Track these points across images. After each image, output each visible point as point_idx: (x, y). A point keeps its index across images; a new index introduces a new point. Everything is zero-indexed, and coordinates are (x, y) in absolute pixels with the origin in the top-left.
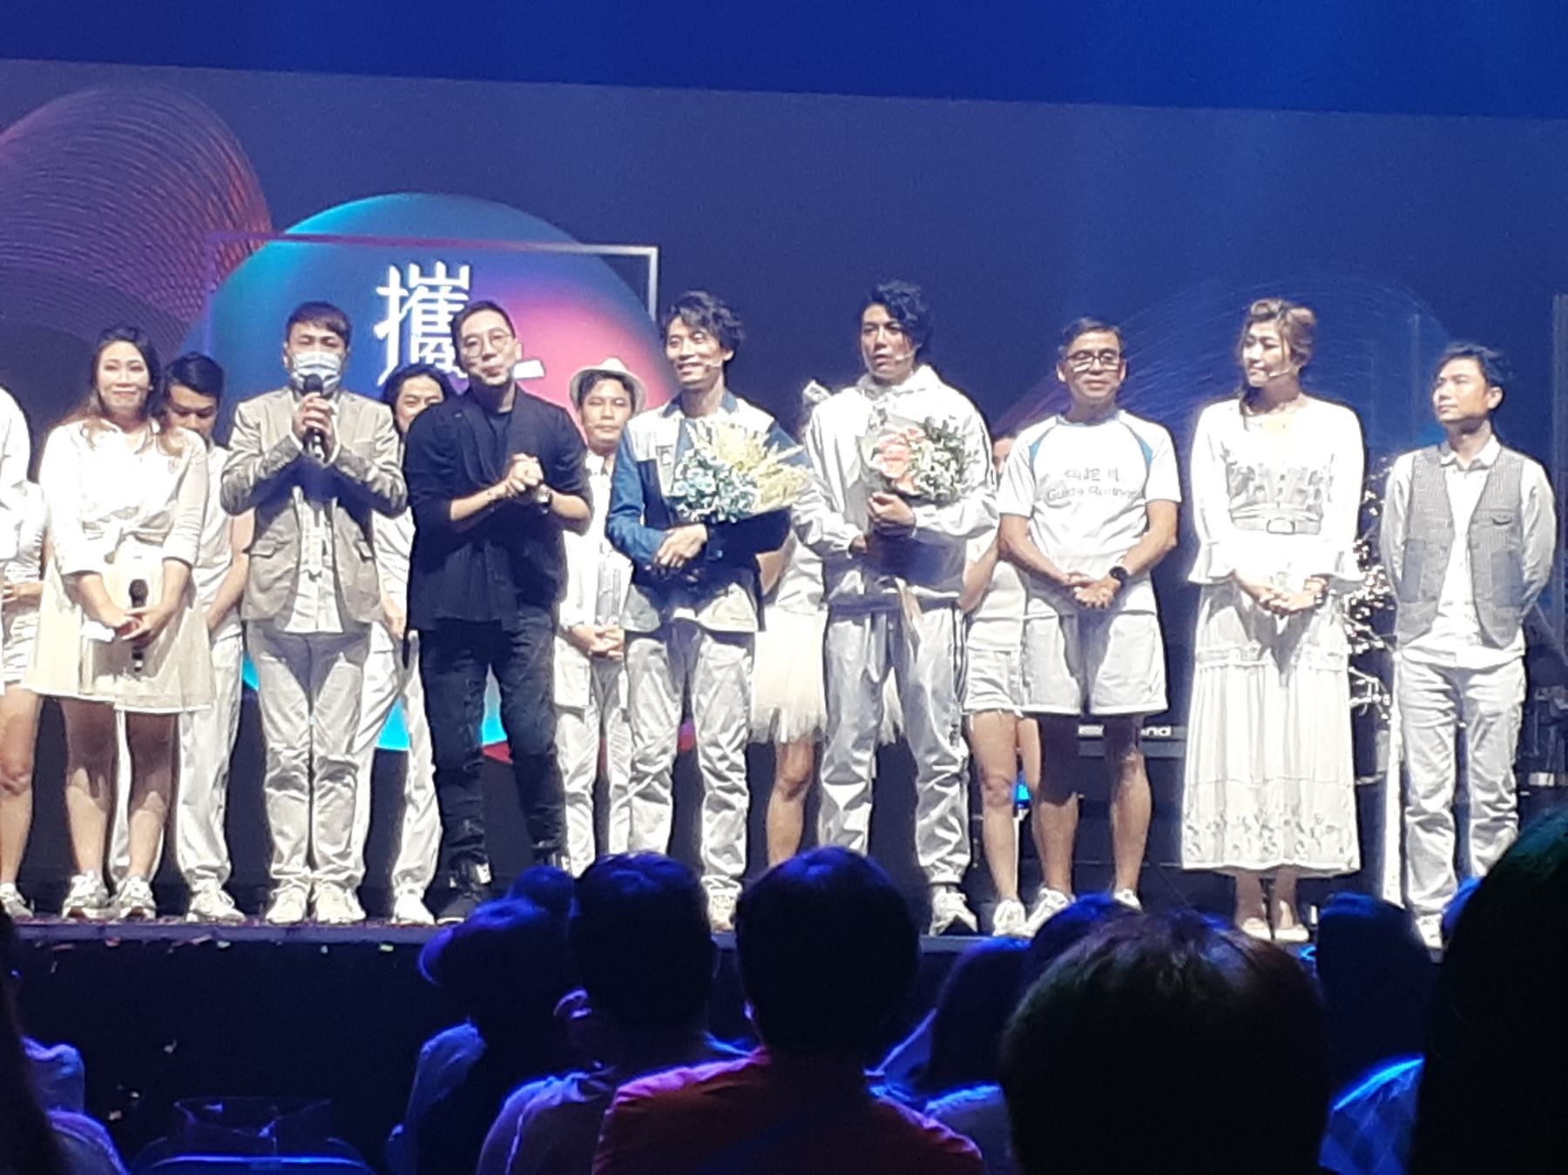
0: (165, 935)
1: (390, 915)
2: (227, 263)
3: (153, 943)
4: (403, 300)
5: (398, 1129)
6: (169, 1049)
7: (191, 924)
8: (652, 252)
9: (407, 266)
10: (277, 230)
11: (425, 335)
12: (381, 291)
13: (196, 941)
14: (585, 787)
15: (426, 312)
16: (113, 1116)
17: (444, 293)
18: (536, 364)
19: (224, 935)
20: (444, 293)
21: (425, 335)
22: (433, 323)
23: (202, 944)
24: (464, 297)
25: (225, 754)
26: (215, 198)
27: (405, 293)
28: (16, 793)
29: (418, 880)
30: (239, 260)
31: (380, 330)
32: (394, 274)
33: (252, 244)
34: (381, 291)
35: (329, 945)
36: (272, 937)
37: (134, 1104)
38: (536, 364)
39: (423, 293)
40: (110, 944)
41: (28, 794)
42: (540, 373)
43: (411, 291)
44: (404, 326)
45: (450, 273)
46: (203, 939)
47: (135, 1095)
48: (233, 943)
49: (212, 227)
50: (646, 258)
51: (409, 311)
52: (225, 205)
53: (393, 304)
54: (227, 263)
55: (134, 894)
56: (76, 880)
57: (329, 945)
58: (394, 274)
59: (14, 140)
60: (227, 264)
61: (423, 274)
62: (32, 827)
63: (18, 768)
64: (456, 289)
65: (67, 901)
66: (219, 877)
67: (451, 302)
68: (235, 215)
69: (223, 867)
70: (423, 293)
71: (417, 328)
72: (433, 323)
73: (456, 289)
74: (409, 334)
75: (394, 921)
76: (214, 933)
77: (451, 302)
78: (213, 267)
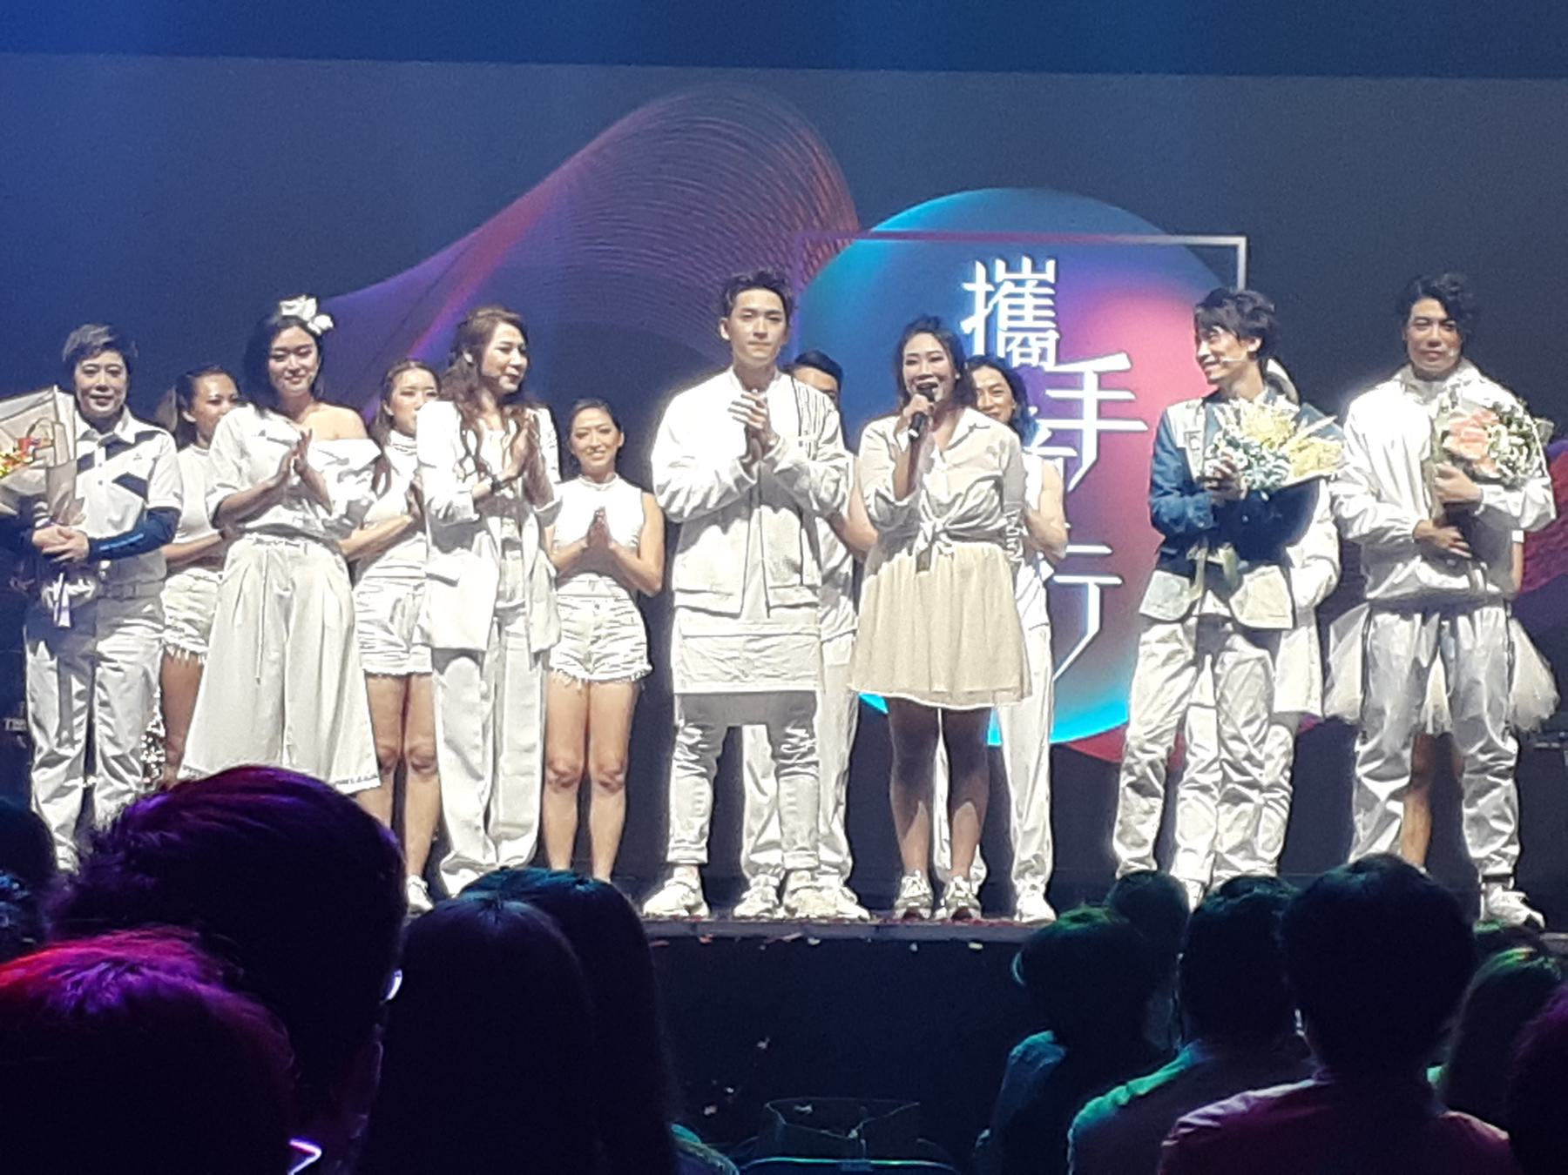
0: (760, 931)
1: (1014, 913)
2: (815, 263)
3: (744, 939)
4: (989, 295)
7: (780, 922)
8: (1241, 242)
12: (967, 287)
13: (788, 938)
15: (1011, 307)
16: (709, 1111)
17: (1030, 287)
18: (1123, 357)
19: (816, 931)
20: (1030, 287)
21: (1011, 329)
24: (1051, 292)
25: (846, 751)
27: (990, 288)
28: (613, 791)
29: (1037, 874)
31: (966, 326)
32: (980, 269)
34: (967, 287)
35: (919, 943)
38: (1123, 357)
39: (1009, 288)
40: (703, 940)
41: (622, 793)
43: (997, 286)
44: (990, 322)
45: (1036, 268)
46: (794, 936)
47: (730, 1090)
48: (824, 941)
49: (798, 222)
50: (1235, 248)
51: (996, 306)
53: (980, 299)
55: (958, 894)
56: (906, 880)
57: (919, 943)
58: (980, 269)
61: (1009, 269)
63: (615, 766)
64: (1042, 284)
65: (898, 902)
66: (842, 874)
67: (1036, 296)
68: (822, 214)
70: (1009, 288)
71: (1003, 322)
73: (1042, 284)
75: (1017, 918)
77: (1036, 296)
78: (801, 266)
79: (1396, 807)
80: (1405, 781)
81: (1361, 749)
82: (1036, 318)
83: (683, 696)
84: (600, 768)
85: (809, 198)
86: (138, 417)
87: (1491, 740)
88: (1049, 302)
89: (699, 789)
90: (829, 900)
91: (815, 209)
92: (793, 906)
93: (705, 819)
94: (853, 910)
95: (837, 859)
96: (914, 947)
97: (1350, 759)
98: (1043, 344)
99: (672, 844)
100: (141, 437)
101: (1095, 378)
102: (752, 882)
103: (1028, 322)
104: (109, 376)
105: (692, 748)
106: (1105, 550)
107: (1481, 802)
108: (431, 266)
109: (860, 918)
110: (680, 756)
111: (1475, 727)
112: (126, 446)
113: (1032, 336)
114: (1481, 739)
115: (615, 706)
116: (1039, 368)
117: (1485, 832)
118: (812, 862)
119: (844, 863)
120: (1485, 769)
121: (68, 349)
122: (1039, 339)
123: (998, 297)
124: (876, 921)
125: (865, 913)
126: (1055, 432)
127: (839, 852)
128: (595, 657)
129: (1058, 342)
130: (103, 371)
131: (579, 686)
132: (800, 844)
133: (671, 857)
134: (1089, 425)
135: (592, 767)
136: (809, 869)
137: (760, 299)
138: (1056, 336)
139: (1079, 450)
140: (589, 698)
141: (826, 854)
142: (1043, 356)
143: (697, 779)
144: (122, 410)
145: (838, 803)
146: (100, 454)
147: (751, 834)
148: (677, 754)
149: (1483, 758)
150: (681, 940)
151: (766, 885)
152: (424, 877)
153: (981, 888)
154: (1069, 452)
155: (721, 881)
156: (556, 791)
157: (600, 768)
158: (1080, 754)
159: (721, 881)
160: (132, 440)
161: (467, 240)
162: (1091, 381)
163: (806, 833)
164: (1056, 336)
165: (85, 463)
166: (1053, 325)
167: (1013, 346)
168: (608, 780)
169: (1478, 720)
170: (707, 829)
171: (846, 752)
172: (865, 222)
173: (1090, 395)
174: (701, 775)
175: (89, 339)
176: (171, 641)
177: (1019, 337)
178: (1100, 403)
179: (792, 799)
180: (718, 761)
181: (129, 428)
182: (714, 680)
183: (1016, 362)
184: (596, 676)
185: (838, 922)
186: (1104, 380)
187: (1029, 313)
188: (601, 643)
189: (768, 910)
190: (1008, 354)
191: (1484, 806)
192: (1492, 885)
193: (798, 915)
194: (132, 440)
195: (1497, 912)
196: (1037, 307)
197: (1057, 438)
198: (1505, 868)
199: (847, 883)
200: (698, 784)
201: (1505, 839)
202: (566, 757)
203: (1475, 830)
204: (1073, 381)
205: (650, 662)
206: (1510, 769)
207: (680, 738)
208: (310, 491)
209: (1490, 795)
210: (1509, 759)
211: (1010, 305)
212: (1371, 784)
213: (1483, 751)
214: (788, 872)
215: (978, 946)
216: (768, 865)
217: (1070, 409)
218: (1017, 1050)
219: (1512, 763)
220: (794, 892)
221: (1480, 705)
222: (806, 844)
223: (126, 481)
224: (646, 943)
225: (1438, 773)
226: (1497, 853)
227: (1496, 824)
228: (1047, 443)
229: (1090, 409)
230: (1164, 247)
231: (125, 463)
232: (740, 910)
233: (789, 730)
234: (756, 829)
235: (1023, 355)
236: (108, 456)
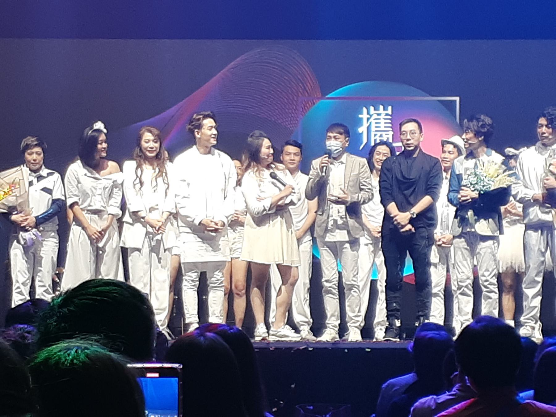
2: (306, 108)
3: (286, 349)
4: (368, 119)
8: (457, 99)
9: (369, 107)
11: (376, 131)
12: (360, 116)
13: (301, 348)
15: (376, 123)
16: (274, 410)
17: (383, 116)
20: (383, 116)
21: (376, 131)
22: (379, 127)
23: (303, 349)
24: (390, 117)
27: (369, 116)
30: (310, 106)
31: (360, 130)
32: (365, 110)
34: (360, 116)
35: (348, 349)
36: (327, 346)
37: (282, 406)
40: (271, 349)
43: (371, 116)
44: (369, 128)
45: (385, 109)
46: (304, 347)
47: (282, 402)
48: (314, 348)
49: (300, 95)
50: (455, 101)
51: (371, 123)
52: (305, 88)
53: (365, 121)
57: (348, 349)
58: (365, 110)
59: (233, 68)
60: (305, 109)
61: (375, 110)
64: (387, 115)
66: (309, 325)
69: (309, 321)
70: (375, 116)
71: (373, 129)
72: (379, 127)
73: (387, 115)
74: (371, 131)
76: (308, 345)
78: (301, 110)
82: (385, 127)
85: (304, 87)
86: (47, 167)
88: (390, 121)
96: (346, 351)
98: (388, 136)
100: (49, 174)
103: (382, 128)
104: (37, 156)
112: (44, 177)
113: (384, 133)
121: (23, 144)
123: (371, 120)
129: (393, 135)
130: (35, 154)
137: (209, 122)
138: (393, 133)
144: (41, 167)
146: (35, 180)
148: (185, 283)
160: (46, 176)
163: (219, 311)
164: (393, 133)
165: (31, 183)
166: (391, 129)
172: (324, 94)
175: (30, 142)
177: (379, 134)
179: (215, 299)
181: (44, 172)
188: (235, 244)
190: (375, 140)
194: (46, 176)
196: (385, 123)
215: (369, 350)
218: (384, 386)
223: (45, 190)
224: (254, 350)
231: (44, 183)
236: (38, 181)
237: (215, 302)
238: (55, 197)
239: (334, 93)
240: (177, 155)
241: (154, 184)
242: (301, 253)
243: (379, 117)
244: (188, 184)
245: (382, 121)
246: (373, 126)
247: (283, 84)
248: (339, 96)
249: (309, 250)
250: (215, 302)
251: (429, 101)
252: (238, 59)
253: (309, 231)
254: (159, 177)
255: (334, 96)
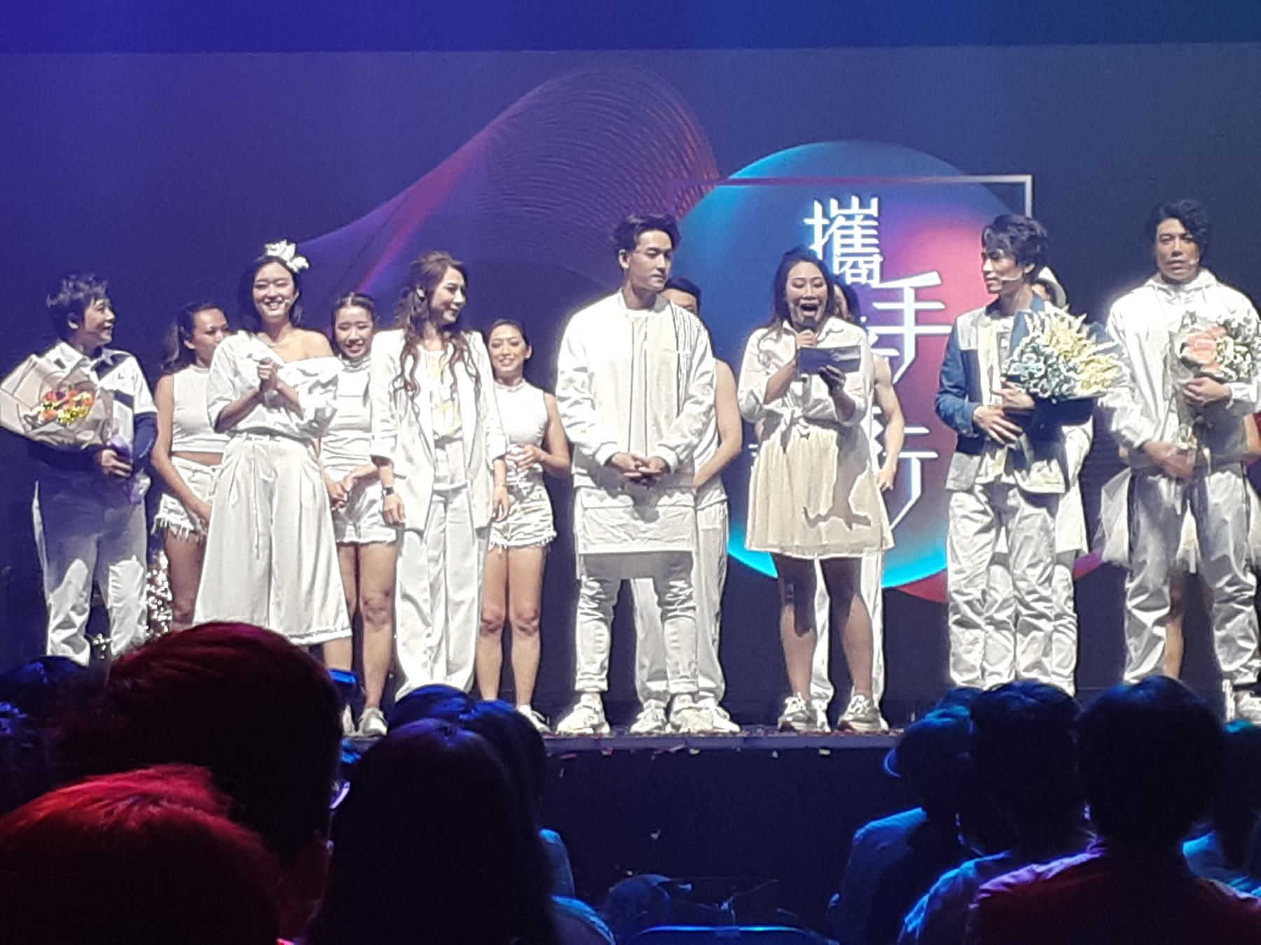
0: (654, 746)
2: (685, 205)
4: (825, 228)
5: (836, 897)
6: (655, 836)
7: (666, 737)
8: (1027, 180)
9: (828, 202)
10: (723, 179)
11: (843, 255)
12: (808, 221)
14: (1009, 617)
15: (843, 237)
17: (858, 221)
20: (858, 221)
21: (843, 255)
22: (851, 246)
23: (678, 751)
24: (875, 223)
26: (673, 153)
27: (826, 222)
28: (530, 634)
32: (818, 207)
33: (703, 188)
34: (808, 221)
35: (777, 750)
39: (841, 221)
40: (605, 753)
41: (537, 635)
42: (938, 282)
43: (832, 220)
45: (863, 205)
50: (1023, 185)
53: (818, 232)
54: (685, 205)
57: (777, 750)
58: (818, 207)
61: (841, 206)
62: (541, 659)
63: (532, 615)
64: (867, 217)
66: (716, 697)
67: (864, 227)
70: (841, 221)
71: (837, 250)
72: (851, 246)
73: (867, 217)
77: (864, 227)
79: (1160, 631)
80: (1166, 611)
81: (1130, 586)
82: (864, 245)
83: (585, 556)
84: (519, 616)
87: (1236, 576)
88: (874, 232)
89: (598, 631)
90: (707, 718)
91: (684, 163)
92: (678, 722)
93: (606, 655)
94: (726, 726)
95: (711, 685)
96: (775, 754)
97: (1123, 594)
98: (870, 266)
99: (579, 676)
101: (912, 292)
102: (645, 705)
105: (592, 598)
106: (924, 430)
107: (1229, 626)
108: (376, 216)
109: (731, 732)
110: (584, 606)
111: (1223, 565)
113: (861, 260)
114: (1226, 574)
115: (529, 565)
116: (867, 285)
117: (1233, 651)
118: (693, 688)
119: (718, 687)
120: (1232, 599)
122: (866, 262)
123: (833, 229)
124: (745, 734)
125: (736, 728)
126: (881, 337)
127: (712, 679)
128: (511, 527)
129: (882, 264)
131: (500, 551)
132: (682, 673)
133: (578, 686)
134: (909, 331)
135: (512, 616)
136: (690, 693)
139: (900, 348)
140: (508, 559)
141: (704, 682)
142: (870, 276)
143: (602, 624)
145: (714, 641)
147: (643, 667)
148: (581, 603)
149: (1229, 590)
150: (585, 753)
151: (657, 707)
152: (381, 708)
153: (829, 705)
154: (894, 352)
155: (620, 702)
156: (485, 635)
157: (519, 616)
158: (905, 594)
159: (620, 702)
161: (402, 195)
162: (909, 295)
163: (686, 664)
166: (877, 250)
167: (846, 268)
168: (526, 626)
169: (1225, 558)
170: (606, 664)
171: (716, 598)
173: (909, 306)
174: (600, 619)
176: (174, 522)
177: (850, 260)
178: (918, 312)
179: (675, 637)
180: (614, 608)
182: (609, 542)
183: (849, 280)
184: (513, 543)
185: (713, 736)
186: (920, 294)
187: (857, 241)
188: (516, 516)
189: (658, 728)
191: (1232, 629)
192: (1241, 693)
193: (682, 730)
195: (1246, 715)
196: (864, 236)
197: (883, 342)
198: (1251, 678)
199: (721, 704)
200: (599, 628)
201: (1250, 654)
202: (494, 609)
203: (1225, 649)
204: (894, 295)
205: (555, 528)
206: (1250, 597)
207: (583, 591)
208: (284, 401)
209: (1235, 620)
210: (1250, 590)
211: (844, 234)
212: (1138, 614)
213: (1229, 584)
214: (673, 696)
216: (658, 693)
217: (893, 318)
218: (860, 832)
219: (1252, 593)
220: (678, 712)
221: (1226, 545)
222: (688, 674)
225: (1192, 603)
226: (1244, 666)
227: (1242, 643)
228: (876, 345)
229: (909, 317)
230: (964, 185)
232: (635, 728)
233: (672, 583)
234: (647, 662)
235: (854, 275)
237: (675, 644)
238: (138, 410)
239: (744, 170)
240: (577, 310)
241: (449, 379)
242: (701, 534)
243: (849, 223)
244: (591, 376)
245: (858, 232)
246: (837, 242)
247: (632, 152)
248: (756, 177)
249: (718, 526)
250: (675, 644)
251: (950, 185)
252: (529, 95)
253: (719, 484)
254: (458, 360)
255: (747, 177)
